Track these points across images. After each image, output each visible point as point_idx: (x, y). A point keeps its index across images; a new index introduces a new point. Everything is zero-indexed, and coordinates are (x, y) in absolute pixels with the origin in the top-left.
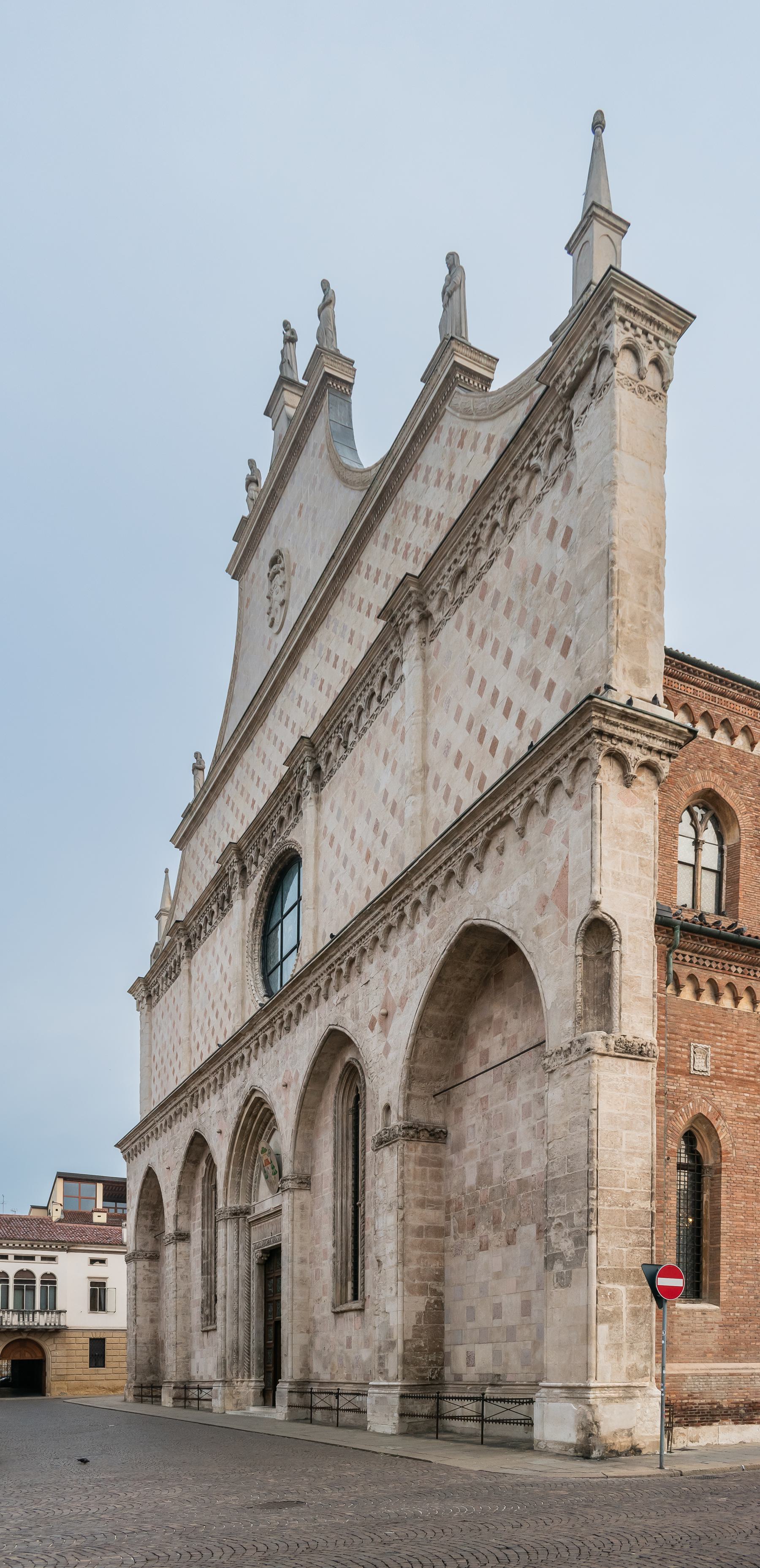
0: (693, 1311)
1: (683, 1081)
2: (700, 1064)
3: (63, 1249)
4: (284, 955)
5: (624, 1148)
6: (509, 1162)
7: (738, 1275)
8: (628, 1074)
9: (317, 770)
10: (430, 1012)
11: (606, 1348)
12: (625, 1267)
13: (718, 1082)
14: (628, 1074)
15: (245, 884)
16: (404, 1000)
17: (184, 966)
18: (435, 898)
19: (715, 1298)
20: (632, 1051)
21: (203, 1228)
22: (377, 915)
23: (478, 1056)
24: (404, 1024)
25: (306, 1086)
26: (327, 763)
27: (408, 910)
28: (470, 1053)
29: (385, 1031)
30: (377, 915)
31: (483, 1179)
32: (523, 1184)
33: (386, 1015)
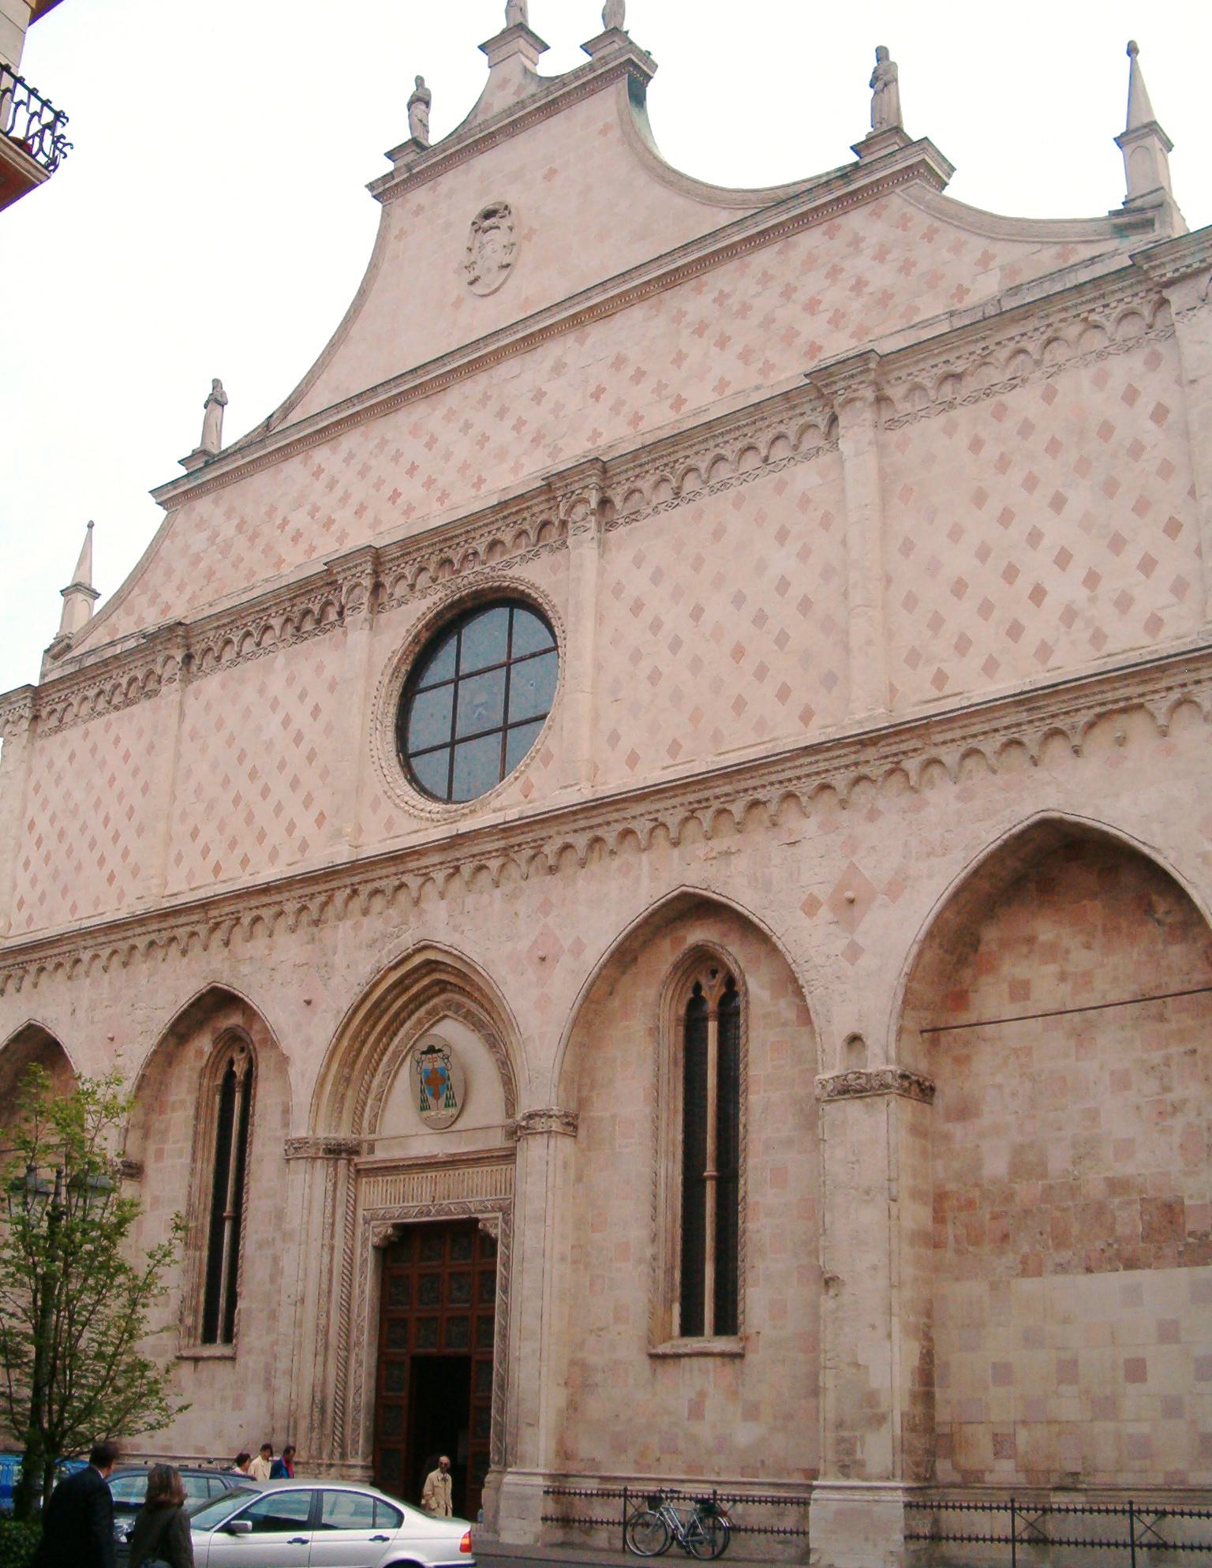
6: (1085, 1151)
9: (605, 502)
16: (895, 888)
18: (970, 763)
21: (194, 1160)
22: (839, 756)
23: (1005, 987)
24: (903, 923)
26: (626, 499)
27: (912, 765)
28: (986, 981)
29: (851, 926)
30: (839, 756)
31: (1026, 1164)
32: (1116, 1186)
33: (852, 901)
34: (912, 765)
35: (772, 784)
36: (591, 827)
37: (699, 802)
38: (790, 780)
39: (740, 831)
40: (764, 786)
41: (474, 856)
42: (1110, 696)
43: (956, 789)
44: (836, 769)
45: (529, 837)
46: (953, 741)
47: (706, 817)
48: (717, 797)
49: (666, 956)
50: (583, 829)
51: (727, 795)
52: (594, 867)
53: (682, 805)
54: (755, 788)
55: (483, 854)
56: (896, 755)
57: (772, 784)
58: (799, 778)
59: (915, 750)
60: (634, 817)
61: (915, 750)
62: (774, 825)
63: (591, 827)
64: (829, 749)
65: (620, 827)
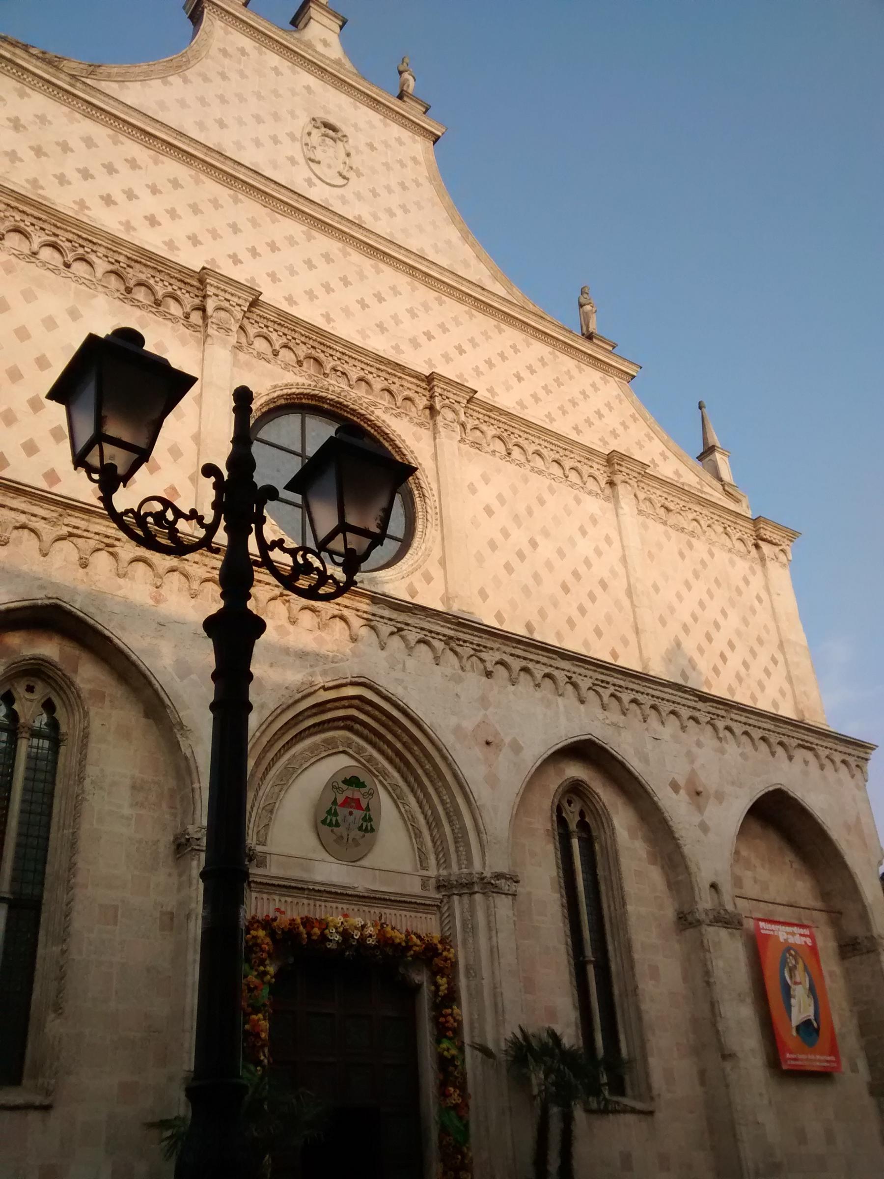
34: (720, 724)
35: (648, 694)
36: (525, 659)
37: (602, 681)
38: (658, 698)
39: (624, 714)
40: (642, 693)
41: (422, 629)
42: (806, 737)
43: (740, 750)
44: (684, 705)
45: (476, 640)
46: (740, 722)
47: (606, 694)
48: (614, 685)
49: (554, 782)
50: (519, 657)
51: (620, 686)
52: (520, 688)
53: (591, 677)
54: (637, 692)
55: (431, 632)
56: (713, 714)
57: (648, 694)
58: (663, 699)
59: (723, 717)
60: (557, 668)
61: (723, 717)
62: (645, 721)
63: (525, 659)
64: (685, 692)
65: (548, 670)
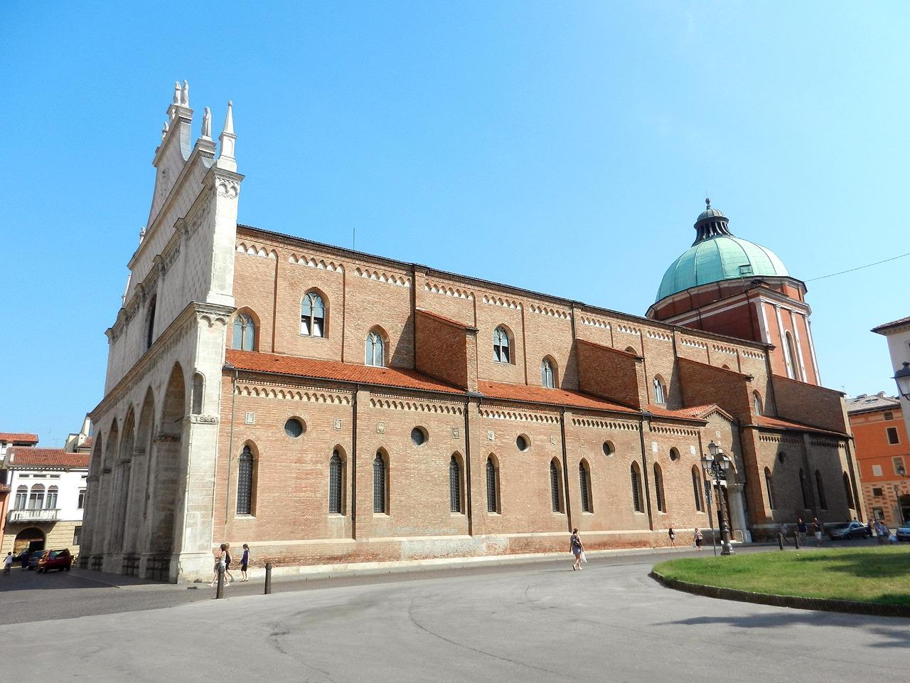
0: (243, 520)
1: (242, 427)
2: (250, 420)
3: (65, 471)
4: (154, 339)
5: (202, 458)
7: (266, 504)
8: (206, 429)
10: (171, 389)
11: (189, 538)
12: (200, 504)
13: (258, 427)
14: (206, 429)
15: (144, 301)
17: (125, 330)
19: (254, 515)
20: (211, 422)
25: (143, 407)
